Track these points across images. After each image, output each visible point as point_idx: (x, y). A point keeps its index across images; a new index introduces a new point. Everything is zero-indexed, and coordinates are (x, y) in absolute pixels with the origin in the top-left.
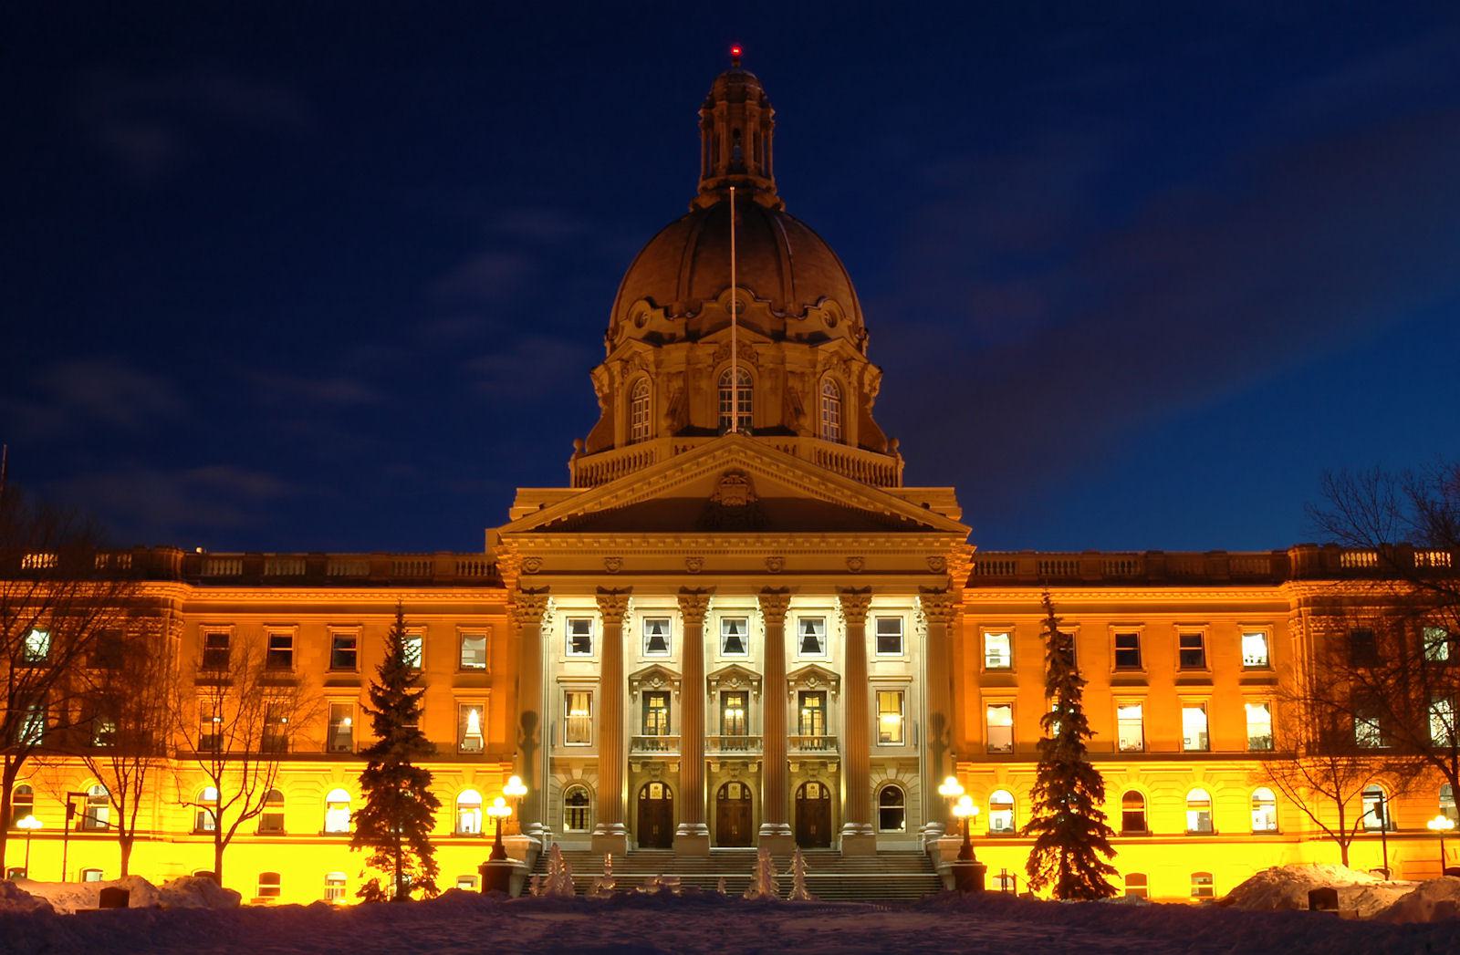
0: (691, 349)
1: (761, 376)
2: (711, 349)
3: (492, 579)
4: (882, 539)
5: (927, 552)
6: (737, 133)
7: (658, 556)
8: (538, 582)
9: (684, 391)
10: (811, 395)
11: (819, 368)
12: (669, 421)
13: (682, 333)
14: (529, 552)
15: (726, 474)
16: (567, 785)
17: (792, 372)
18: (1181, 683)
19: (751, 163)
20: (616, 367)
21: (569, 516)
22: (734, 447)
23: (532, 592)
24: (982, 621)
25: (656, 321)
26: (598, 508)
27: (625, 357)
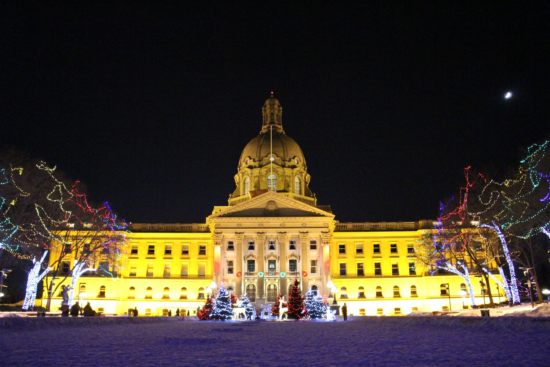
0: (260, 169)
1: (279, 177)
2: (266, 170)
3: (208, 231)
5: (323, 222)
6: (272, 114)
7: (251, 223)
8: (219, 230)
9: (259, 181)
10: (292, 182)
11: (294, 175)
12: (254, 189)
13: (258, 165)
14: (217, 222)
15: (270, 202)
16: (227, 285)
18: (391, 257)
19: (276, 121)
20: (241, 175)
21: (228, 213)
22: (271, 194)
23: (218, 233)
24: (338, 241)
25: (251, 162)
26: (235, 211)
27: (243, 172)
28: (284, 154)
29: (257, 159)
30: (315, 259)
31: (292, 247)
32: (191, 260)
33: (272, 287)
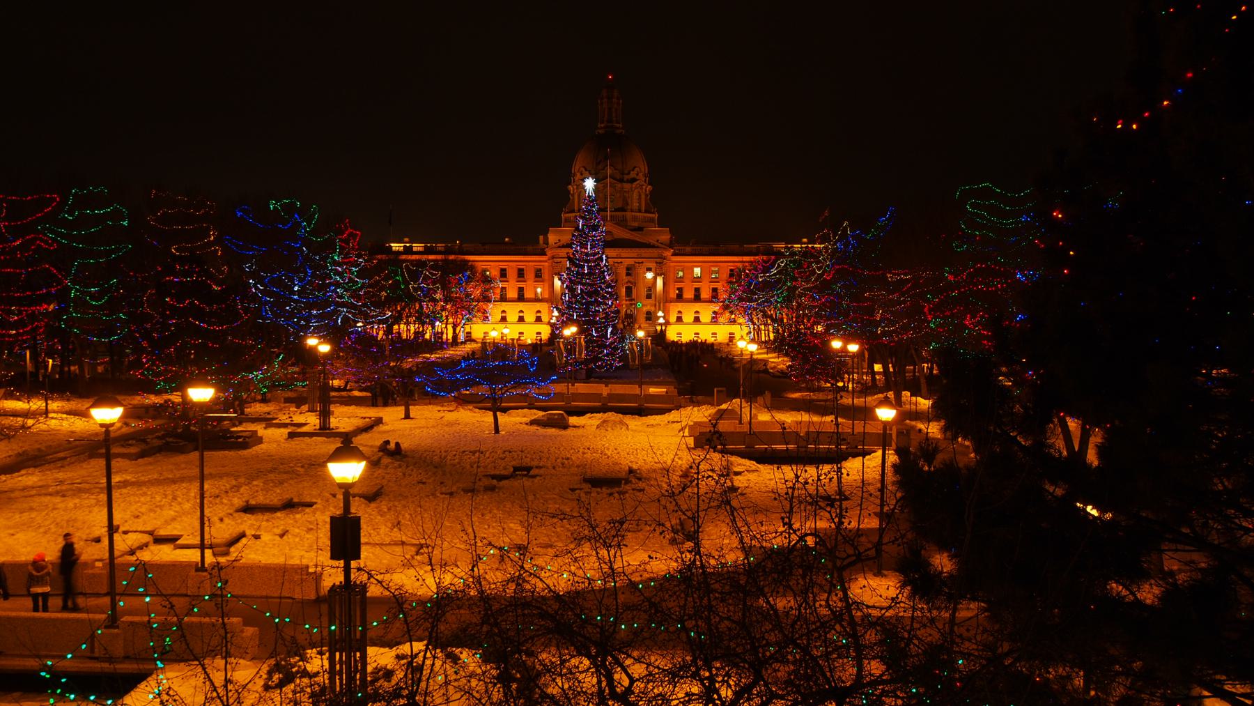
2: (602, 185)
8: (559, 260)
17: (625, 192)
19: (614, 119)
20: (575, 187)
23: (557, 263)
30: (650, 285)
32: (528, 283)
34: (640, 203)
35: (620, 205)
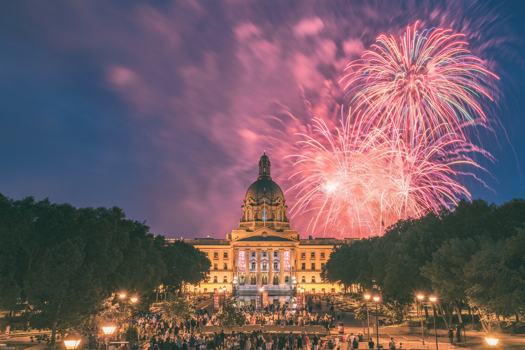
2: (261, 207)
4: (285, 242)
8: (237, 248)
9: (257, 213)
13: (256, 204)
15: (264, 232)
20: (246, 208)
23: (236, 249)
25: (252, 201)
28: (272, 197)
29: (256, 200)
31: (275, 255)
32: (220, 260)
33: (265, 277)
34: (281, 217)
35: (270, 218)
